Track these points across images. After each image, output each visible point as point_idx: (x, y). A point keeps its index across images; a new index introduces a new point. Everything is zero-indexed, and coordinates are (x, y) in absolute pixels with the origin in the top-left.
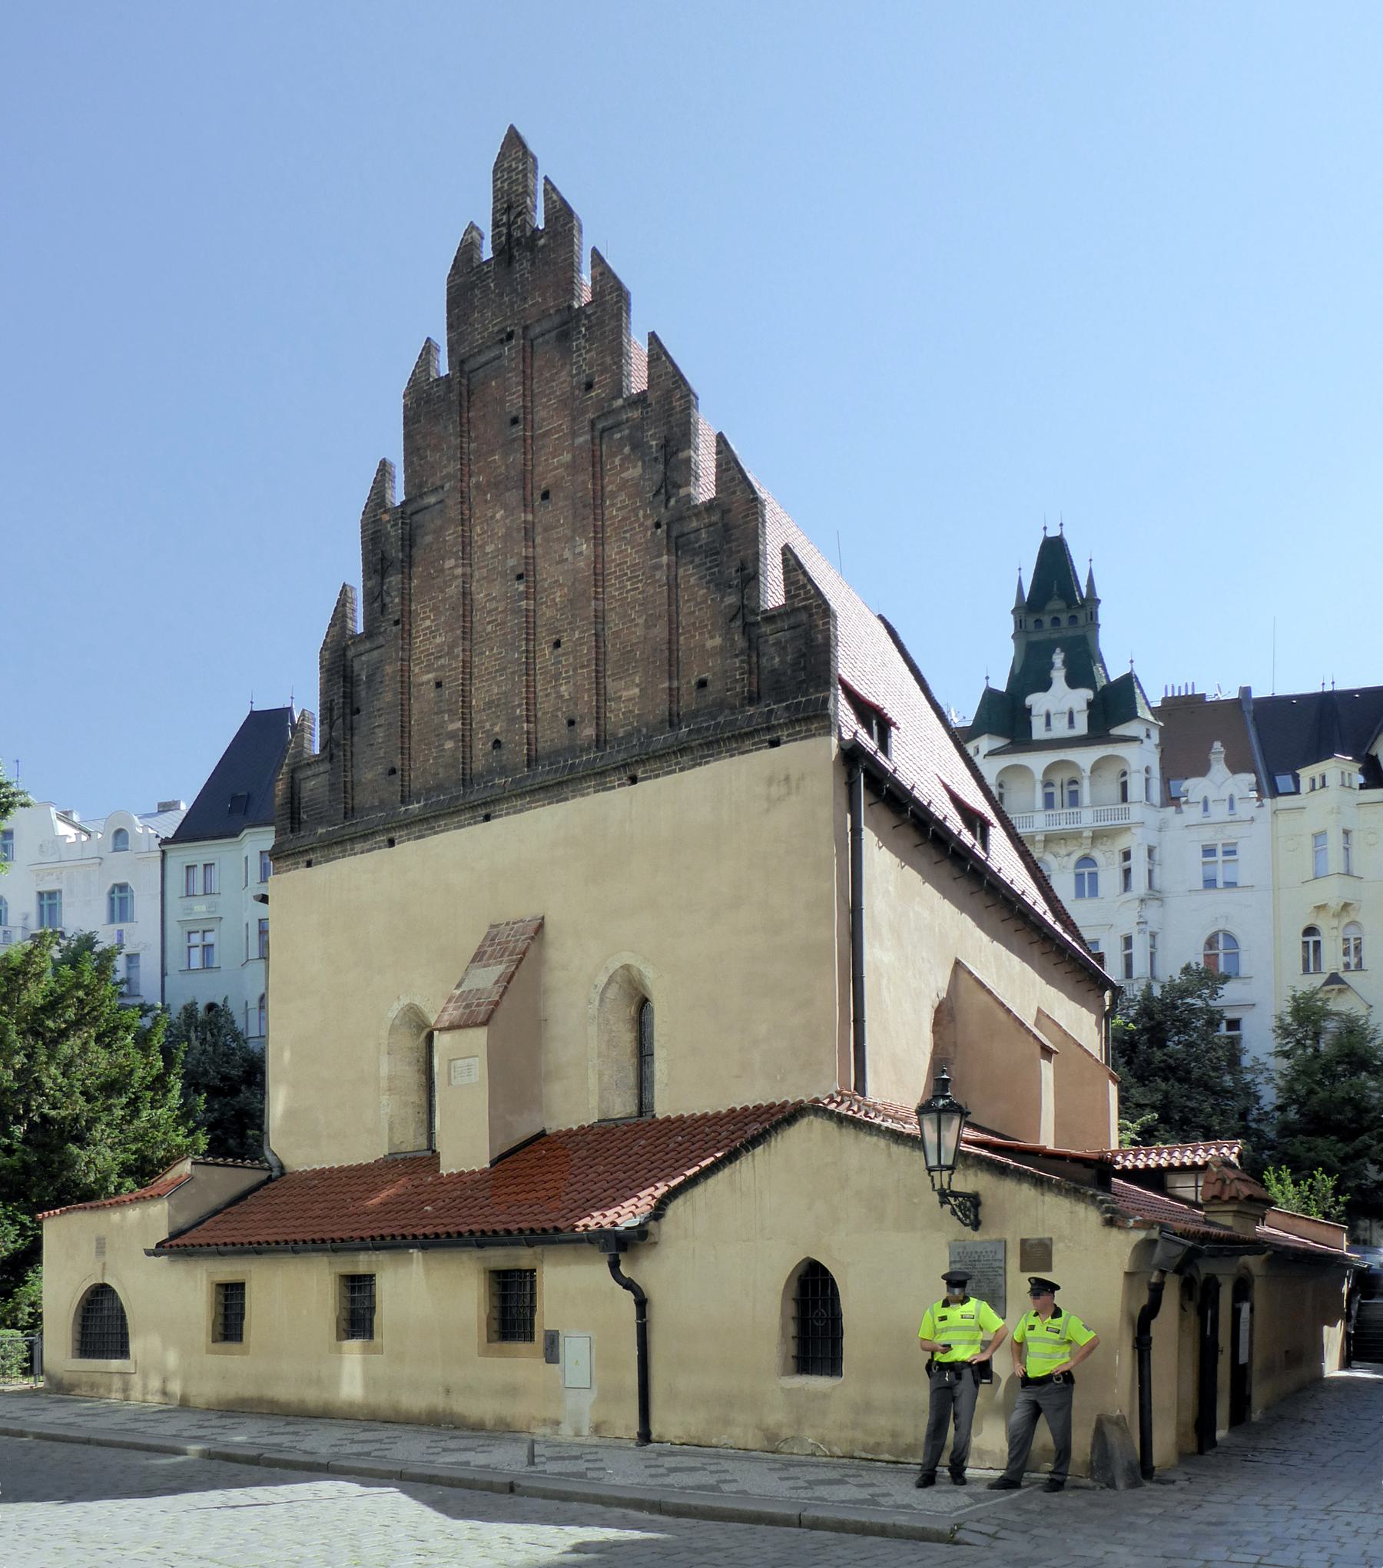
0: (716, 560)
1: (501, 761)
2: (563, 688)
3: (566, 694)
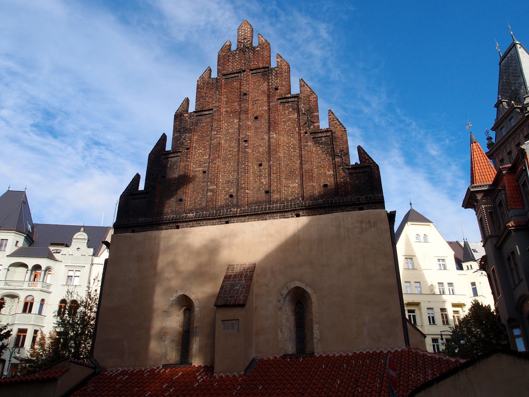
0: (329, 147)
1: (233, 202)
2: (263, 180)
3: (265, 183)
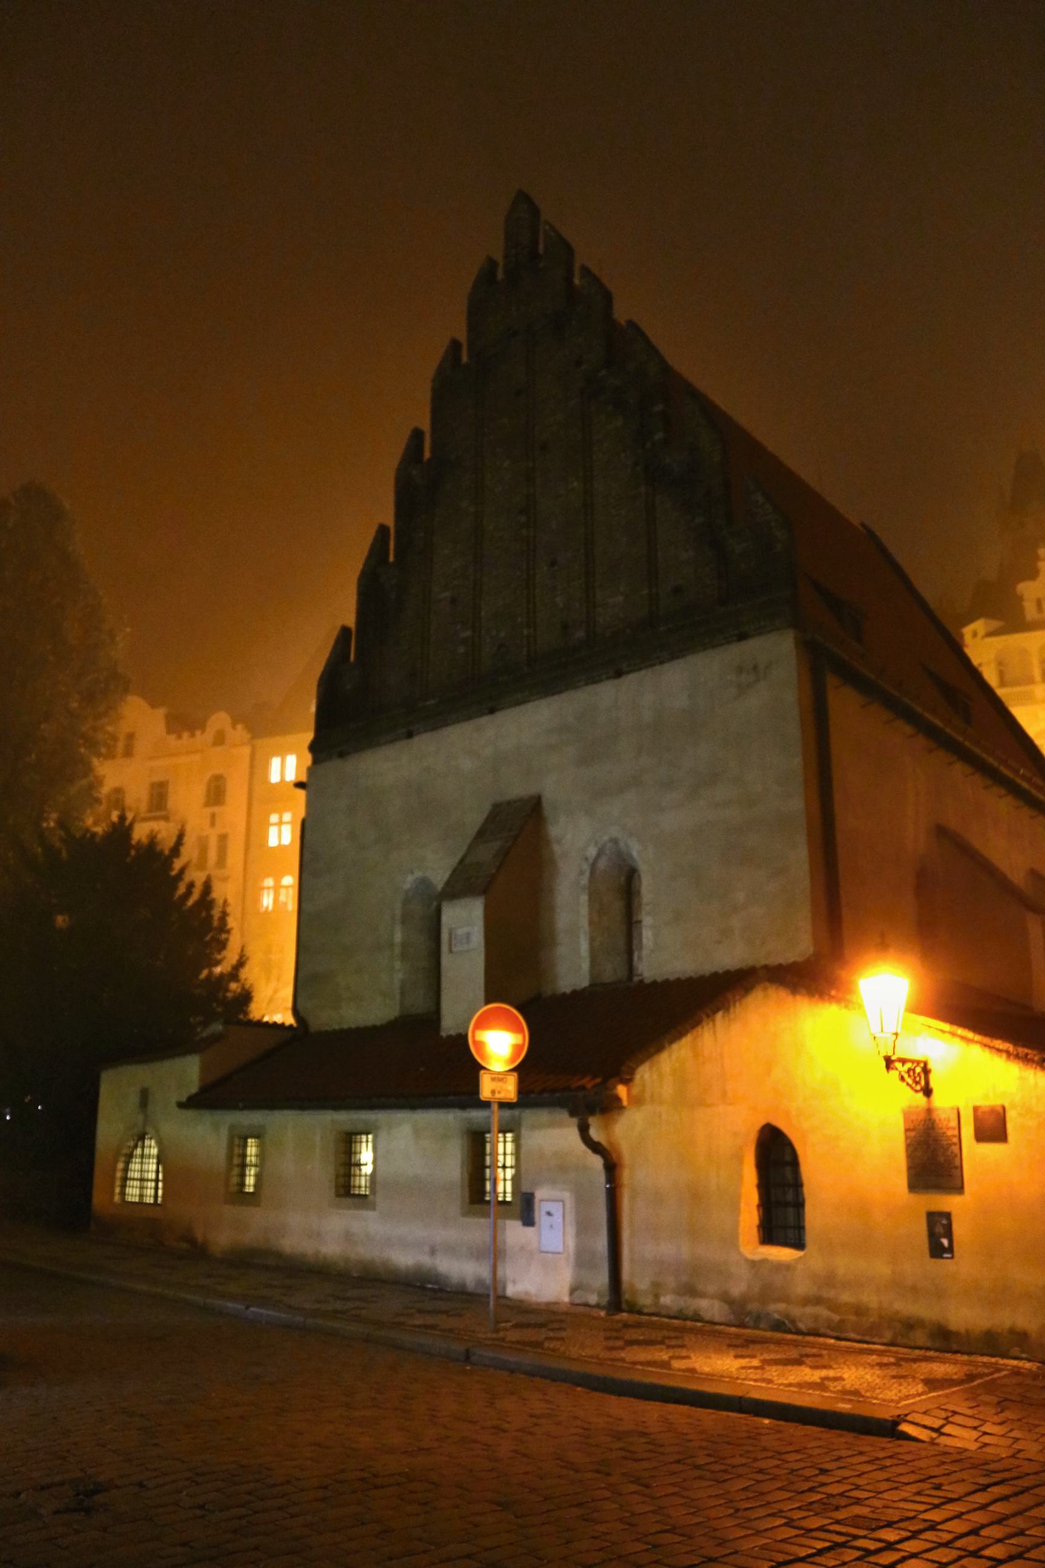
2: (558, 599)
